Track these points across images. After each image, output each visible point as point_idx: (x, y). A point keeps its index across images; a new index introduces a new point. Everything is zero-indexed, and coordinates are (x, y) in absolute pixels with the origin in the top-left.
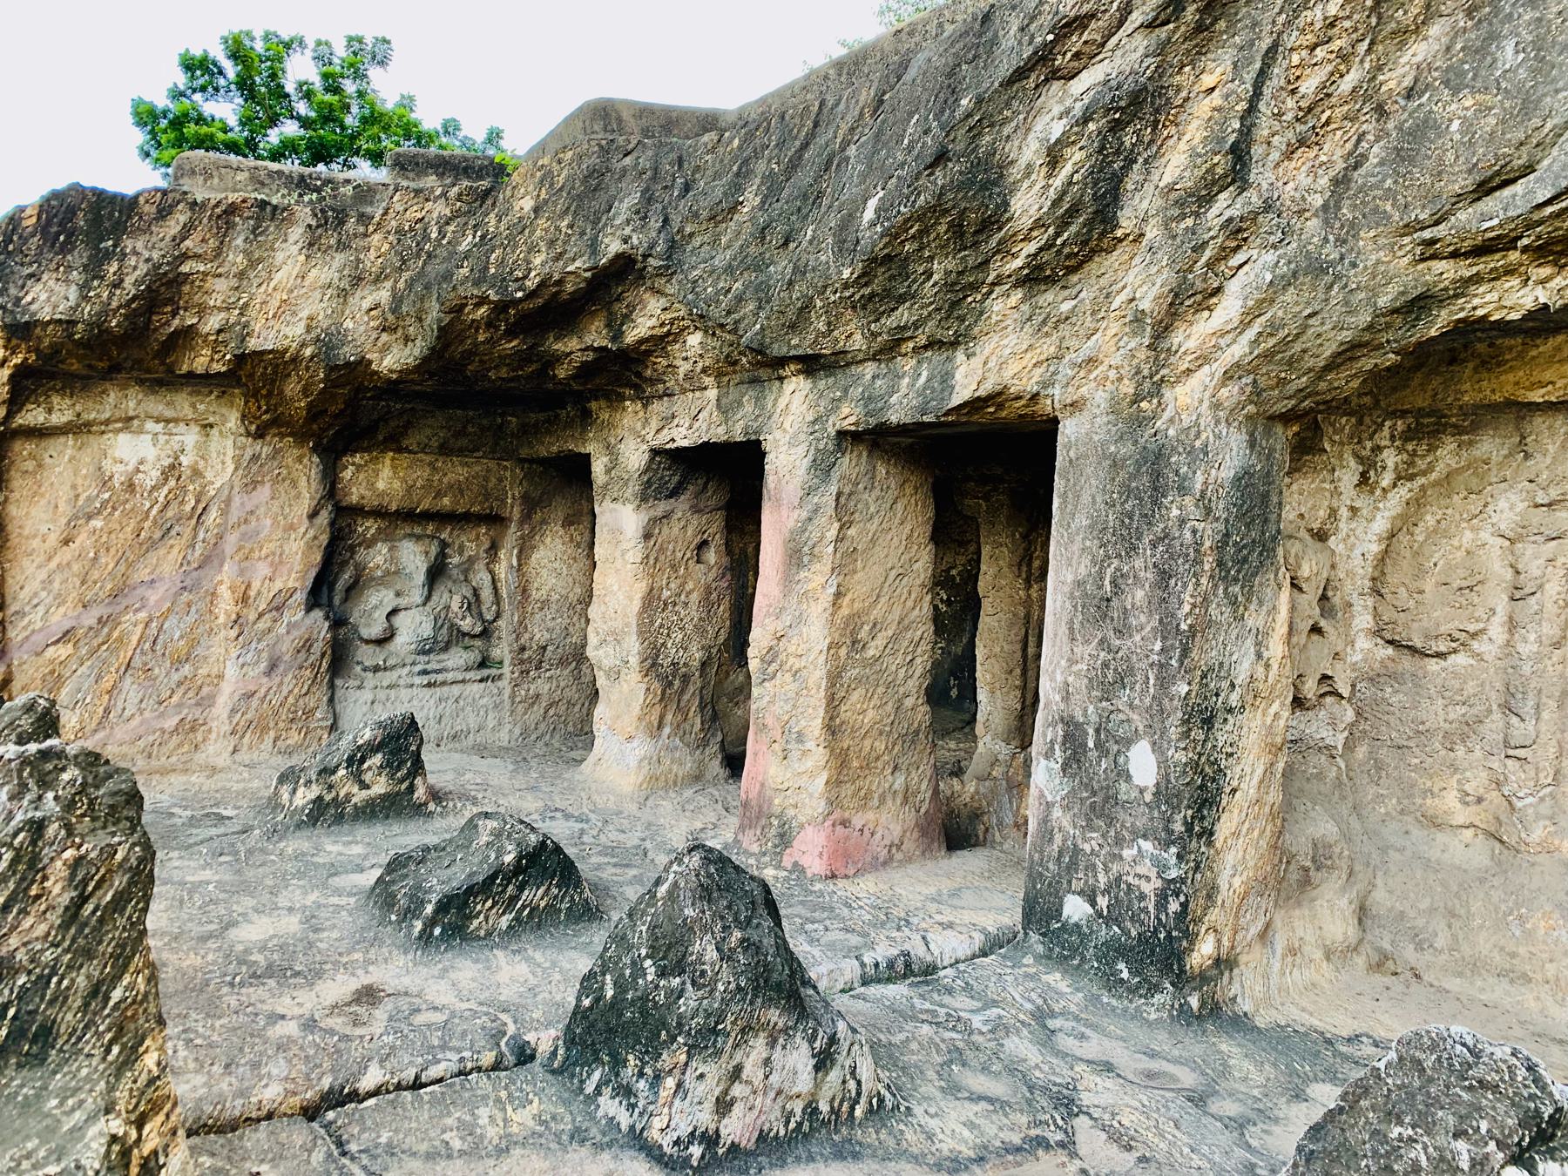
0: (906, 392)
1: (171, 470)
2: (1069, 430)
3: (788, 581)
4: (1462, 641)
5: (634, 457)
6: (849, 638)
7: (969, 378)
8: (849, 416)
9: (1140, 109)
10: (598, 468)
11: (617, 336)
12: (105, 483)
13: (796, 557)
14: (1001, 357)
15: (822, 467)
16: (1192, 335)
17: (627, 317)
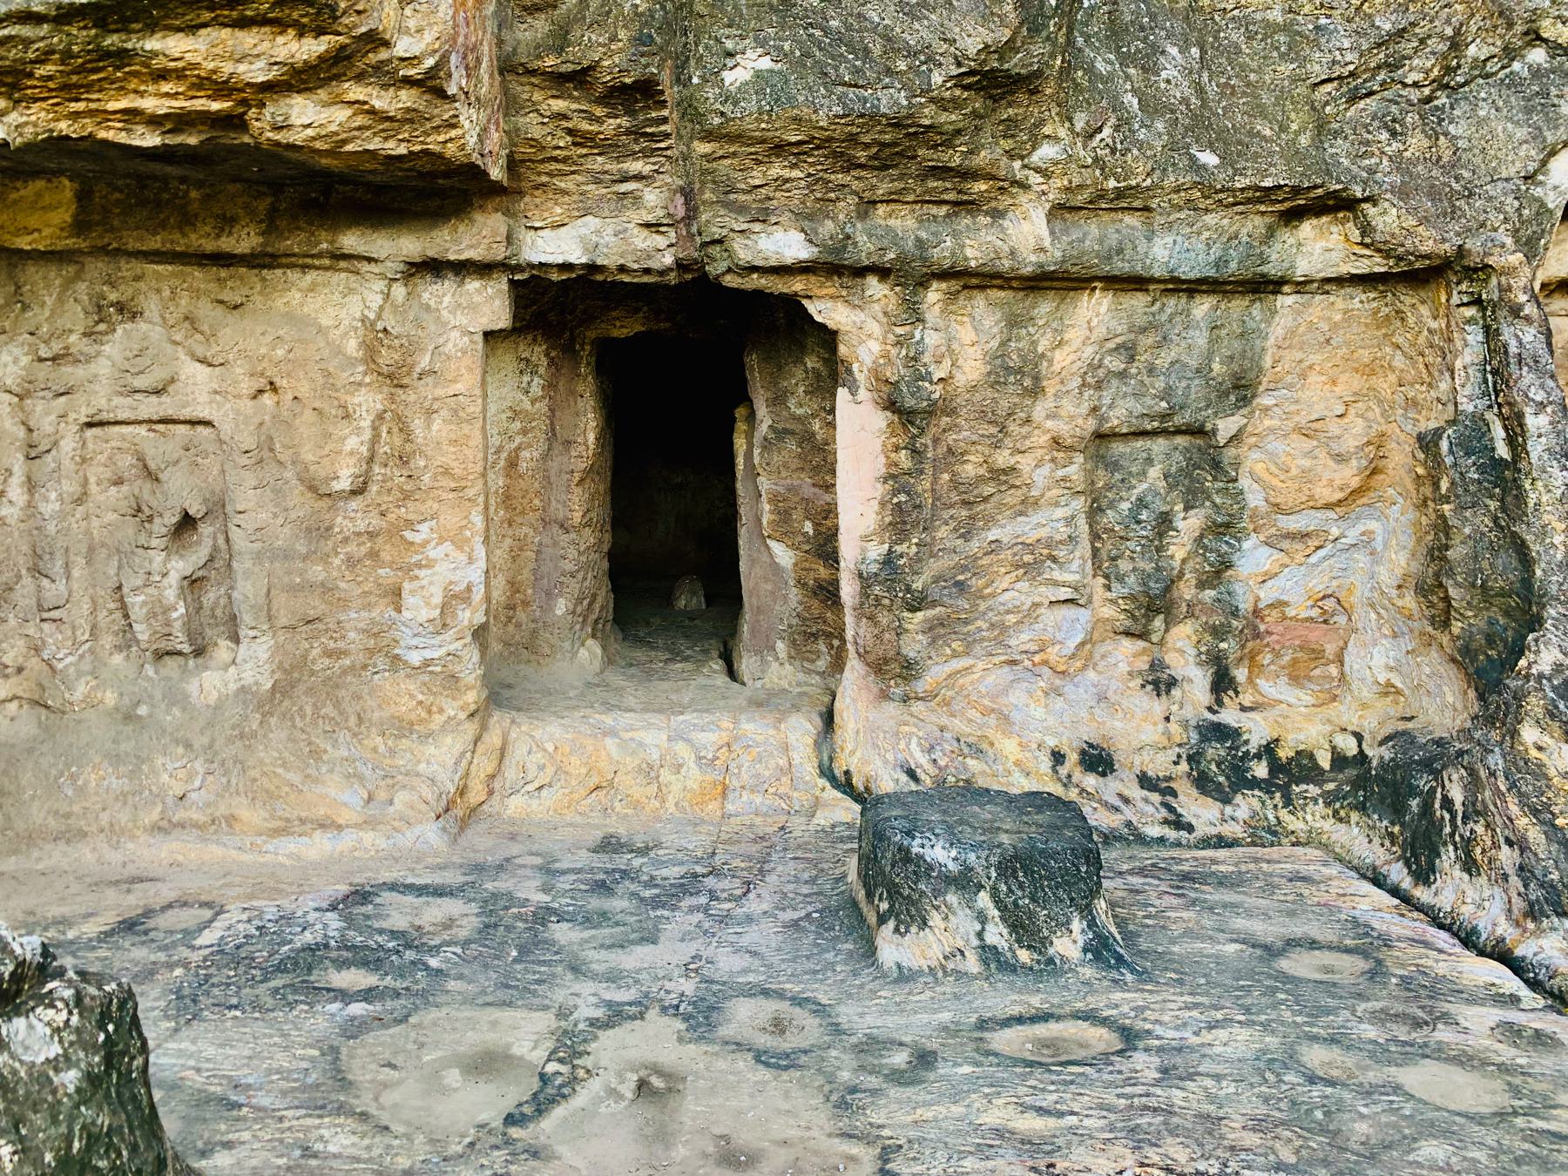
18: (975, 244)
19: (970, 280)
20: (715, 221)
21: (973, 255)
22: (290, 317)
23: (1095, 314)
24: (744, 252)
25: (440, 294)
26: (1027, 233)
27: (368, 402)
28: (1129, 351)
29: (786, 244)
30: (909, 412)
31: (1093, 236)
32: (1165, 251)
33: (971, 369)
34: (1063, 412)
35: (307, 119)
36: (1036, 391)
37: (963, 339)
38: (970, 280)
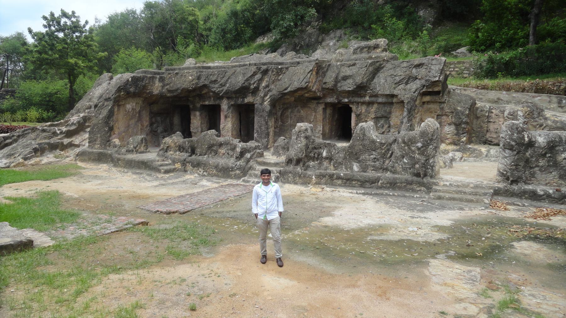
0: (240, 101)
1: (133, 109)
2: (256, 105)
3: (225, 120)
4: (287, 122)
5: (198, 105)
6: (233, 126)
7: (246, 101)
8: (233, 103)
9: (261, 80)
10: (191, 106)
11: (201, 92)
12: (126, 111)
13: (226, 117)
14: (249, 99)
15: (229, 108)
16: (266, 98)
17: (203, 90)
18: (362, 100)
19: (363, 103)
20: (341, 98)
21: (362, 101)
22: (310, 107)
23: (376, 106)
24: (343, 101)
25: (319, 105)
26: (367, 98)
27: (314, 114)
28: (379, 109)
29: (346, 100)
30: (358, 116)
31: (373, 99)
32: (380, 100)
33: (363, 111)
34: (373, 116)
35: (306, 95)
36: (369, 113)
37: (363, 109)
38: (363, 103)
